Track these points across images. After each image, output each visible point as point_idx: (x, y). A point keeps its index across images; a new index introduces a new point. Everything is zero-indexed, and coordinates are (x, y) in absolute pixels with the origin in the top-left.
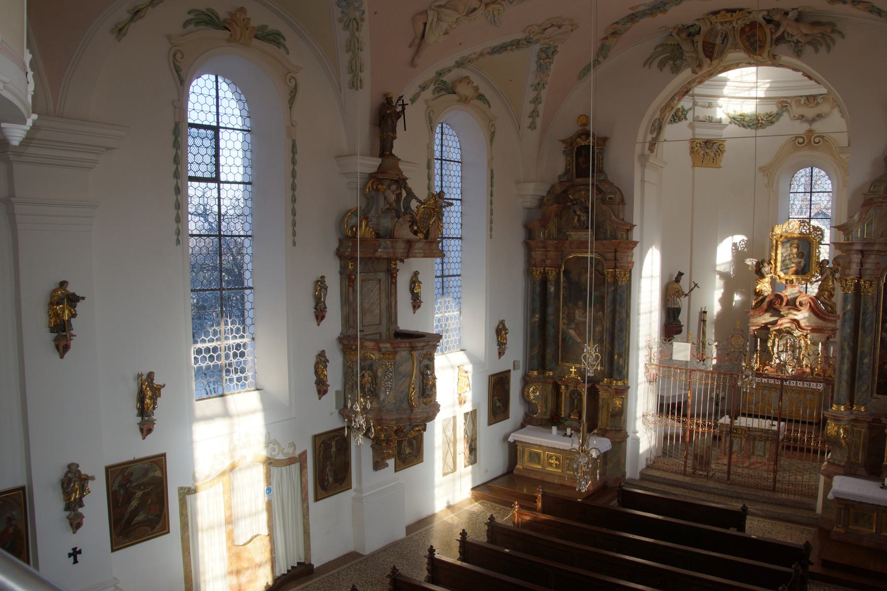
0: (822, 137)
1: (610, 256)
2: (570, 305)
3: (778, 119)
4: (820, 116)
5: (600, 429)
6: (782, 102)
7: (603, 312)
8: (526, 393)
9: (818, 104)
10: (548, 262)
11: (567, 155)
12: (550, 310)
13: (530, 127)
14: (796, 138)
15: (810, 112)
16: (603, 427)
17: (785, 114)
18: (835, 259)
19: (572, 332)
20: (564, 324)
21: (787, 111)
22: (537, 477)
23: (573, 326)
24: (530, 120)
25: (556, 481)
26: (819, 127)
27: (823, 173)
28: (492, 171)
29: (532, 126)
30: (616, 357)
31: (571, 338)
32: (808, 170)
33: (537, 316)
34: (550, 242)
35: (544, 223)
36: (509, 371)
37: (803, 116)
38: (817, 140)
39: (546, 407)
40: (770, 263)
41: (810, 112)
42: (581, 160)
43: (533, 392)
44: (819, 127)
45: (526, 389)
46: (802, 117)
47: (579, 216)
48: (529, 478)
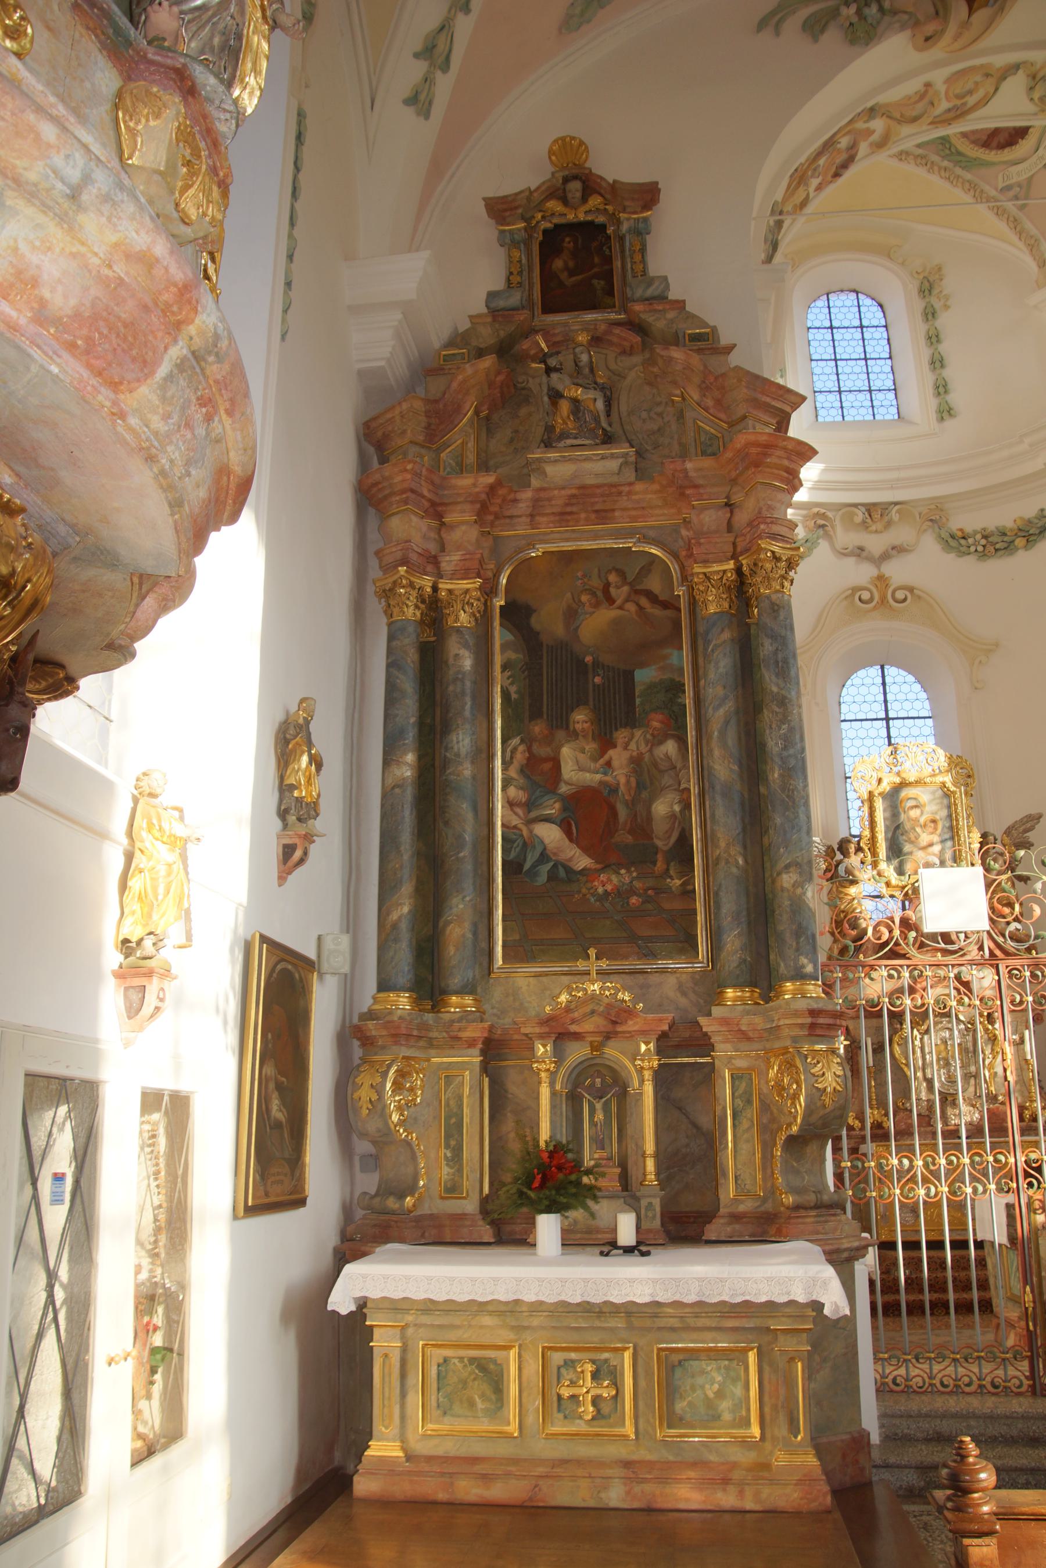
0: (911, 590)
1: (711, 518)
2: (538, 728)
3: (810, 550)
4: (899, 550)
5: (736, 1218)
6: (817, 515)
7: (682, 741)
8: (365, 1094)
9: (889, 524)
10: (450, 561)
11: (514, 244)
12: (462, 741)
13: (412, 100)
14: (855, 590)
15: (876, 543)
16: (746, 1206)
17: (823, 546)
18: (1008, 832)
19: (550, 834)
20: (510, 804)
21: (828, 536)
22: (498, 1492)
23: (553, 808)
24: (421, 67)
25: (615, 1496)
26: (898, 572)
27: (911, 678)
28: (301, 115)
29: (419, 101)
30: (787, 880)
31: (544, 857)
32: (874, 671)
33: (410, 757)
34: (465, 482)
35: (439, 419)
36: (309, 965)
37: (861, 549)
38: (900, 595)
39: (456, 1157)
40: (859, 849)
41: (876, 543)
42: (558, 264)
43: (398, 1087)
44: (898, 572)
45: (366, 1079)
46: (859, 552)
47: (575, 401)
48: (454, 1506)
